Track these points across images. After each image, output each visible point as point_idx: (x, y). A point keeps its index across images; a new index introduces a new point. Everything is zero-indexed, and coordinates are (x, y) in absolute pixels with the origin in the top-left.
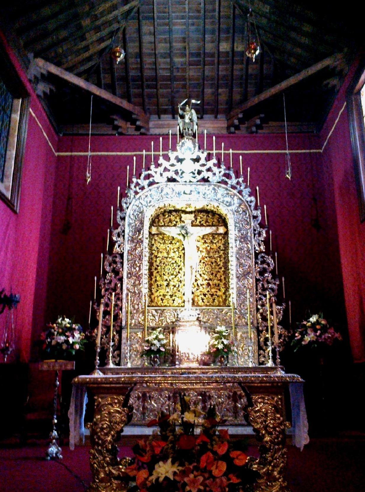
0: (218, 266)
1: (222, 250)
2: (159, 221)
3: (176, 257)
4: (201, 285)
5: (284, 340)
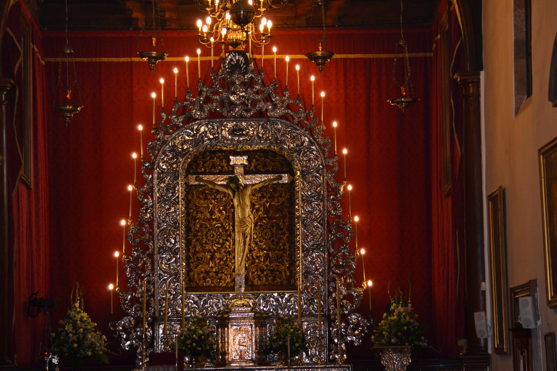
0: (281, 229)
1: (287, 207)
2: (198, 165)
3: (222, 219)
4: (258, 257)
5: (362, 331)
